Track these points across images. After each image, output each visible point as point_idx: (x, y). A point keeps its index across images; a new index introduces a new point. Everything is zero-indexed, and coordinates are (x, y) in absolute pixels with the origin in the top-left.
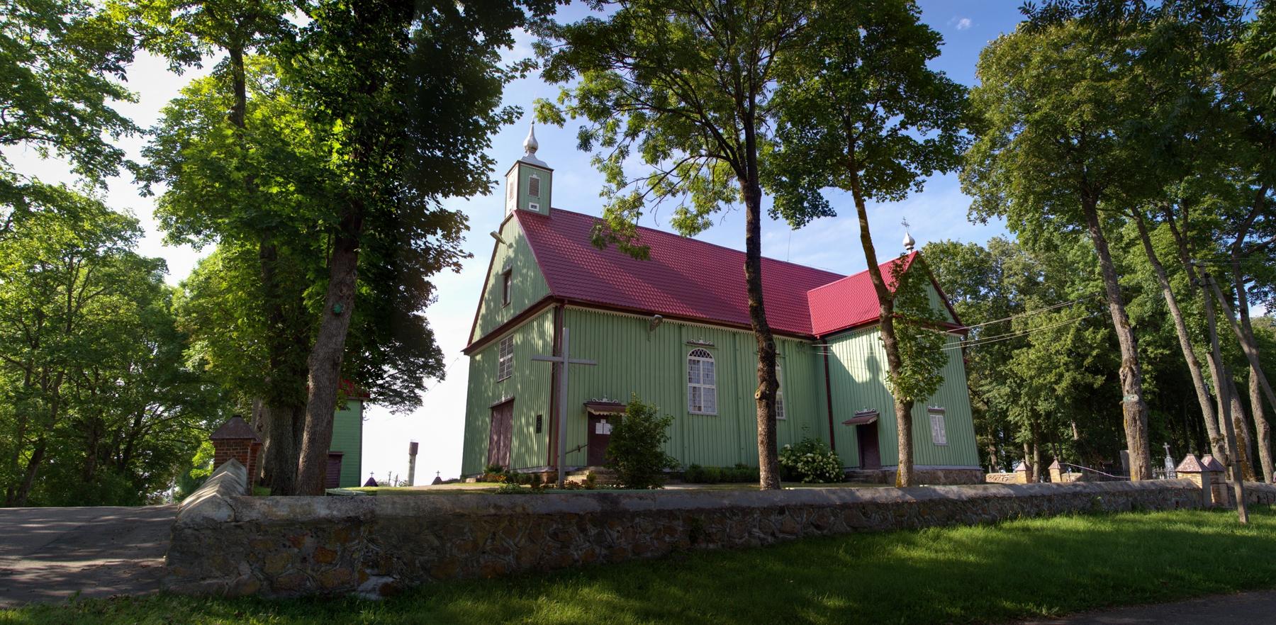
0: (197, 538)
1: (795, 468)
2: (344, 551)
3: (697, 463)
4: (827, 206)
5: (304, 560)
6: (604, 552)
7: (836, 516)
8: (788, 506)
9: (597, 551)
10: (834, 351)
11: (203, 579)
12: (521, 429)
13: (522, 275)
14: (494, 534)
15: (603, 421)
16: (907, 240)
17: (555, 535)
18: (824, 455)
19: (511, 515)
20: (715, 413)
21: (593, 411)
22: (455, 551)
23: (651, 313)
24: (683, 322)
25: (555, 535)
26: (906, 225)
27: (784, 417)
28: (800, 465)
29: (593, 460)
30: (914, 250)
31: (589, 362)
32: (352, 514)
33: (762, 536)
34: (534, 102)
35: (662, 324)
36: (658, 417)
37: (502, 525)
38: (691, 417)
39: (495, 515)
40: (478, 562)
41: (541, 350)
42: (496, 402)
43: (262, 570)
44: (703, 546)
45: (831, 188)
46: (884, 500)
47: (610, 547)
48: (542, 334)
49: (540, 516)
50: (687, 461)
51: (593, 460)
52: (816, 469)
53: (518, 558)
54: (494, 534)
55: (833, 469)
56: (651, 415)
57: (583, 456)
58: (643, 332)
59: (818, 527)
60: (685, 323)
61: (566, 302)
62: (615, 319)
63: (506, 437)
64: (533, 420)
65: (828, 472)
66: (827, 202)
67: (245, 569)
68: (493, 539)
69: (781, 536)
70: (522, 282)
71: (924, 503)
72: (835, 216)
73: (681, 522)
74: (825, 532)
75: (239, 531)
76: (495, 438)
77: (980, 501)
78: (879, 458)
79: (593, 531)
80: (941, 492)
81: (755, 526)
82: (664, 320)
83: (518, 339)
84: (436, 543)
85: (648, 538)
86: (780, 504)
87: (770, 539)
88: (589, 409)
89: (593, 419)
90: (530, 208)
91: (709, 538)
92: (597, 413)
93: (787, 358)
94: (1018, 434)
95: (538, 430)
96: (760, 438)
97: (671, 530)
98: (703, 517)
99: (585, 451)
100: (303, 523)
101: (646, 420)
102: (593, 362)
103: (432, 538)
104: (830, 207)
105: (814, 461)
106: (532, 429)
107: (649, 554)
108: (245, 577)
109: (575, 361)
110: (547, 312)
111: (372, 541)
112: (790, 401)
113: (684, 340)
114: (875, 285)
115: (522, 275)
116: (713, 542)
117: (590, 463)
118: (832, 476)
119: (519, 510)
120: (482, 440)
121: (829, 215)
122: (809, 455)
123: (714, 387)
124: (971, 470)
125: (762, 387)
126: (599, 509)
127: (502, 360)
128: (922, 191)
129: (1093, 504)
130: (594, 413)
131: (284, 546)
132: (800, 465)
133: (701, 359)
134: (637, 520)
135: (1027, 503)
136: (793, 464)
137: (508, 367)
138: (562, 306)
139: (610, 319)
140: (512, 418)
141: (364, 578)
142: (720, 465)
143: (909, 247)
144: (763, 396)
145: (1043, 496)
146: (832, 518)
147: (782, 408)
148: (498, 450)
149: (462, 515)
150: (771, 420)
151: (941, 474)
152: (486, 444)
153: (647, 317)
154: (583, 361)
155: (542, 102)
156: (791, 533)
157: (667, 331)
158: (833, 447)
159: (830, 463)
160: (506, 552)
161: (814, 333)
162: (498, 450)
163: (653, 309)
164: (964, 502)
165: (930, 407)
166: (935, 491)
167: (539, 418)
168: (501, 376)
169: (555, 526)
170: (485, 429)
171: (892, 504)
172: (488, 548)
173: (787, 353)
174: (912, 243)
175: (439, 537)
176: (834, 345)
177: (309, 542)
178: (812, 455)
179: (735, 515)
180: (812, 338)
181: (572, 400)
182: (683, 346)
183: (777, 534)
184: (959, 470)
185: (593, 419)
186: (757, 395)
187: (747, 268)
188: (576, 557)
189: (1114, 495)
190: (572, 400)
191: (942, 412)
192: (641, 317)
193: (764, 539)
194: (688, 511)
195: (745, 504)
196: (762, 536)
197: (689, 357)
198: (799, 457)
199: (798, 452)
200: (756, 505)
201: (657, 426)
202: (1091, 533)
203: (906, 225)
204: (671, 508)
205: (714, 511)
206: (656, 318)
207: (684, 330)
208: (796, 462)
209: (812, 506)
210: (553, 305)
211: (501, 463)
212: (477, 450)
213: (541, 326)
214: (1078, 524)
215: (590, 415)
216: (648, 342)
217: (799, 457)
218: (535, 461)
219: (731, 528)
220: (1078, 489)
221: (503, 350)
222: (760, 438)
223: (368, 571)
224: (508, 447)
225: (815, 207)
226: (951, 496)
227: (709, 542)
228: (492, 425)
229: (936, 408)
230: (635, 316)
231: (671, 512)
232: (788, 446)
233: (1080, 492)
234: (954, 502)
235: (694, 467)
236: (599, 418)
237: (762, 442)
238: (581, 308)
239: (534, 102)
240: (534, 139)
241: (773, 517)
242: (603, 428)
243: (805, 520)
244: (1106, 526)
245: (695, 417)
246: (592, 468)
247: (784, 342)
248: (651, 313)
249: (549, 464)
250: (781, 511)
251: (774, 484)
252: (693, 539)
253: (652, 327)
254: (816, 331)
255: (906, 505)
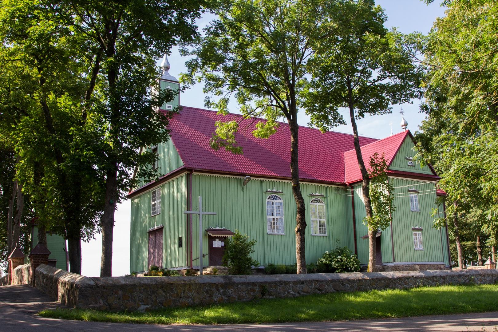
0: (86, 290)
1: (330, 265)
2: (132, 296)
3: (273, 263)
4: (342, 119)
5: (119, 299)
6: (226, 298)
7: (328, 285)
8: (305, 281)
9: (224, 298)
10: (358, 193)
11: (90, 304)
12: (168, 247)
13: (164, 152)
14: (184, 291)
15: (217, 240)
16: (403, 123)
17: (207, 292)
18: (348, 257)
19: (190, 284)
20: (284, 234)
21: (211, 235)
22: (171, 297)
23: (244, 175)
24: (263, 179)
25: (207, 292)
26: (403, 113)
27: (326, 235)
28: (333, 263)
29: (212, 262)
30: (407, 129)
31: (212, 213)
32: (133, 283)
33: (293, 293)
34: (179, 75)
35: (250, 181)
36: (249, 240)
37: (187, 288)
38: (269, 236)
39: (184, 284)
40: (179, 301)
41: (179, 199)
42: (151, 229)
43: (107, 302)
44: (268, 297)
45: (344, 108)
46: (353, 278)
47: (229, 297)
48: (179, 190)
49: (201, 284)
50: (267, 262)
51: (212, 262)
52: (343, 265)
53: (193, 300)
54: (184, 291)
55: (353, 265)
56: (245, 240)
57: (206, 260)
58: (239, 187)
59: (319, 290)
60: (264, 179)
61: (194, 171)
62: (222, 179)
63: (159, 250)
64: (176, 241)
65: (350, 267)
66: (342, 116)
67: (101, 301)
68: (184, 293)
69: (302, 293)
70: (165, 157)
71: (373, 279)
72: (346, 124)
73: (258, 287)
74: (323, 292)
75: (98, 288)
76: (152, 251)
77: (403, 279)
78: (381, 258)
79: (222, 290)
80: (384, 275)
81: (290, 289)
82: (252, 178)
83: (163, 191)
84: (164, 294)
85: (244, 293)
86: (302, 280)
87: (297, 295)
88: (209, 233)
89: (211, 239)
90: (167, 108)
91: (270, 294)
92: (214, 236)
93: (329, 198)
94: (488, 240)
95: (180, 245)
96: (297, 251)
97: (254, 291)
98: (267, 285)
99: (207, 257)
100: (118, 286)
101: (242, 242)
102: (214, 213)
103: (162, 292)
104: (343, 119)
105: (342, 260)
106: (176, 246)
107: (245, 300)
108: (102, 304)
109: (205, 213)
110: (182, 176)
111: (140, 293)
112: (330, 224)
113: (264, 190)
114: (361, 170)
115: (164, 152)
116: (272, 295)
117: (211, 264)
118: (353, 269)
119: (192, 282)
120: (143, 252)
121: (343, 123)
122: (339, 257)
123: (283, 218)
124: (437, 265)
125: (298, 226)
126: (224, 282)
127: (153, 203)
128: (391, 113)
129: (470, 280)
130: (212, 235)
131: (113, 294)
132: (333, 263)
133: (275, 201)
134: (239, 286)
135: (430, 280)
136: (329, 263)
137: (158, 208)
138: (191, 173)
139: (219, 179)
140: (162, 239)
141: (139, 306)
142: (287, 264)
143: (404, 127)
144: (299, 231)
145: (441, 276)
146: (327, 286)
147: (325, 229)
148: (155, 257)
149: (172, 284)
150: (302, 241)
151: (417, 267)
152: (146, 254)
153: (241, 177)
154: (209, 213)
155: (183, 74)
156: (307, 292)
157: (254, 185)
158: (356, 253)
159: (351, 262)
160: (189, 297)
161: (345, 182)
162: (155, 257)
163: (245, 172)
164: (394, 279)
165: (413, 227)
166: (380, 274)
167: (180, 239)
168: (154, 213)
169: (206, 288)
170: (145, 245)
171: (357, 280)
172: (182, 296)
173: (328, 195)
174: (406, 125)
175: (164, 292)
176: (358, 189)
177: (120, 293)
178: (341, 257)
179: (281, 284)
180: (344, 185)
181: (199, 228)
182: (264, 194)
183: (301, 292)
184: (430, 265)
185: (211, 239)
186: (296, 230)
187: (292, 166)
188: (216, 300)
189: (484, 276)
190: (199, 228)
191: (421, 230)
192: (238, 177)
193: (294, 295)
194: (261, 283)
195: (286, 280)
196: (293, 293)
197: (267, 200)
198: (333, 258)
199: (333, 256)
200: (291, 280)
201: (248, 245)
202: (464, 292)
203: (403, 113)
204: (253, 281)
205: (272, 283)
206: (247, 178)
207: (264, 184)
208: (331, 261)
209: (317, 281)
210: (185, 173)
211: (156, 265)
212: (140, 258)
213: (178, 185)
214: (454, 289)
215: (210, 236)
216: (242, 192)
217: (333, 258)
218: (178, 264)
219: (280, 290)
220: (462, 273)
221: (153, 197)
222: (297, 251)
223: (140, 303)
224: (161, 257)
225: (335, 119)
226: (389, 276)
227: (270, 295)
228: (149, 243)
229: (417, 227)
230: (234, 177)
231: (253, 283)
232: (327, 252)
233: (463, 275)
234: (389, 279)
235: (271, 265)
236: (214, 238)
237: (298, 252)
238: (202, 174)
239: (179, 75)
240: (168, 62)
241: (298, 285)
242: (218, 244)
243: (313, 287)
244: (470, 289)
245: (272, 237)
246: (212, 267)
247: (326, 188)
248: (244, 175)
249: (187, 265)
250: (303, 283)
251: (303, 272)
252: (263, 294)
253: (245, 183)
254: (347, 181)
255: (363, 281)
